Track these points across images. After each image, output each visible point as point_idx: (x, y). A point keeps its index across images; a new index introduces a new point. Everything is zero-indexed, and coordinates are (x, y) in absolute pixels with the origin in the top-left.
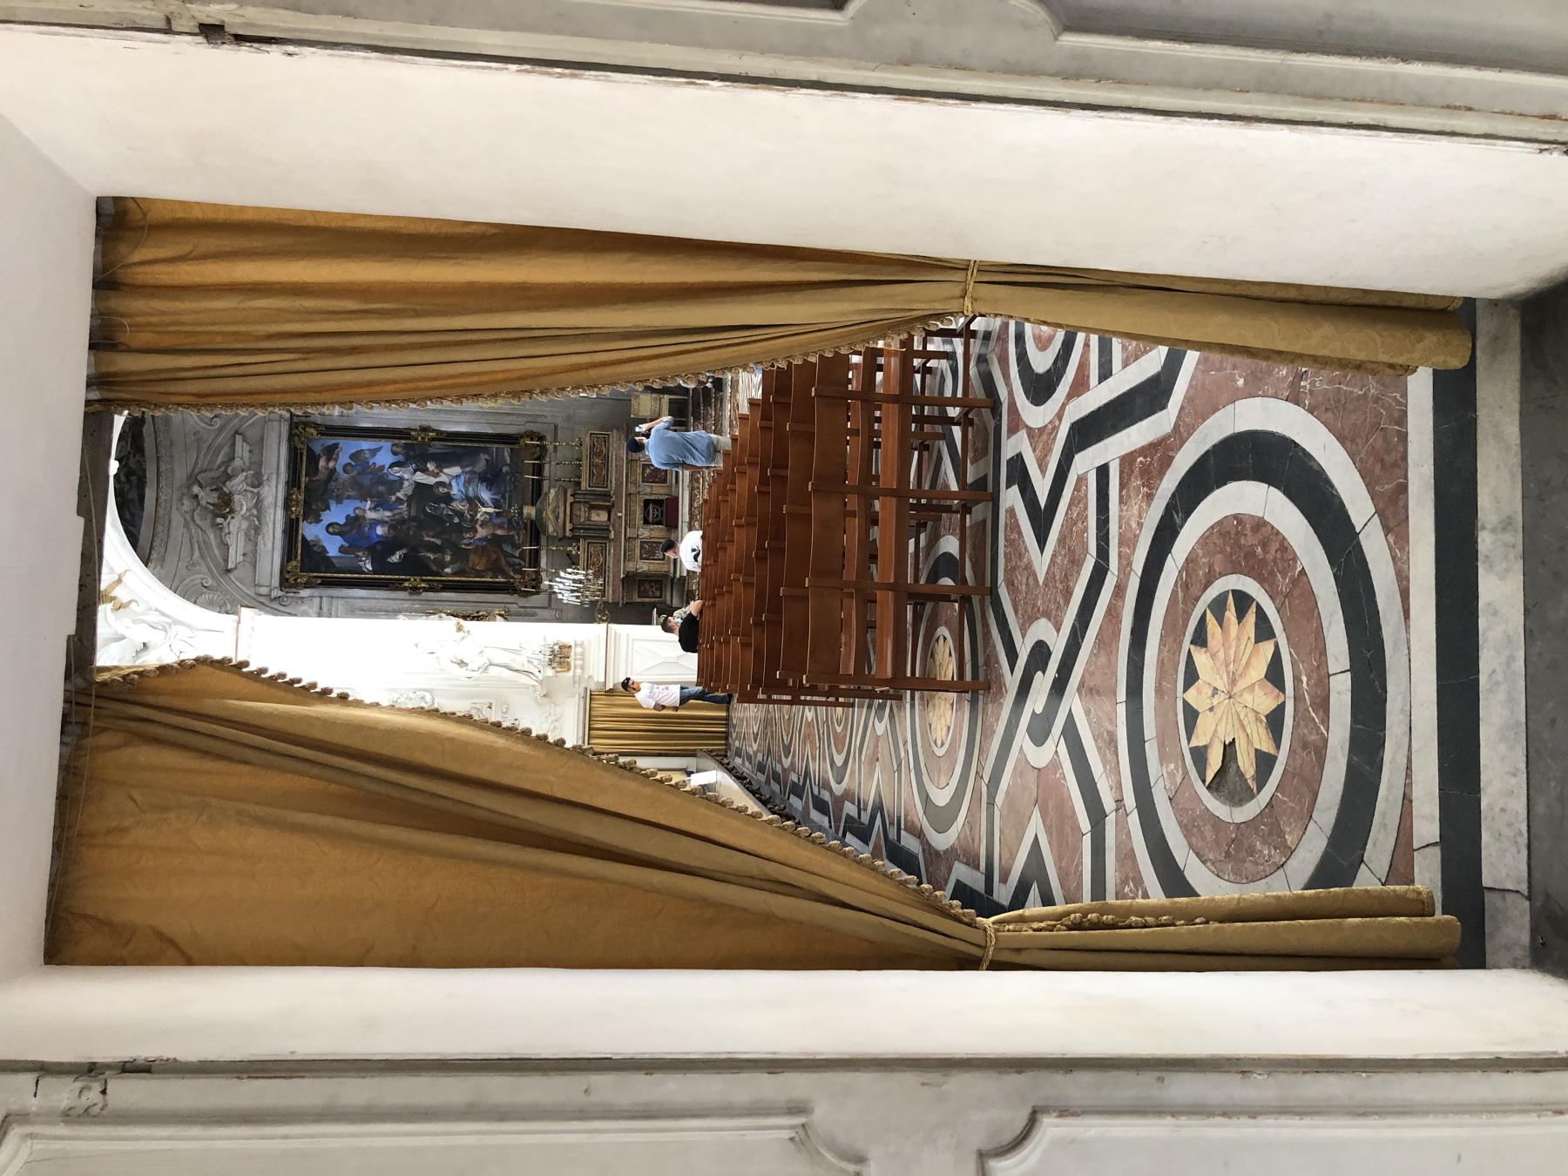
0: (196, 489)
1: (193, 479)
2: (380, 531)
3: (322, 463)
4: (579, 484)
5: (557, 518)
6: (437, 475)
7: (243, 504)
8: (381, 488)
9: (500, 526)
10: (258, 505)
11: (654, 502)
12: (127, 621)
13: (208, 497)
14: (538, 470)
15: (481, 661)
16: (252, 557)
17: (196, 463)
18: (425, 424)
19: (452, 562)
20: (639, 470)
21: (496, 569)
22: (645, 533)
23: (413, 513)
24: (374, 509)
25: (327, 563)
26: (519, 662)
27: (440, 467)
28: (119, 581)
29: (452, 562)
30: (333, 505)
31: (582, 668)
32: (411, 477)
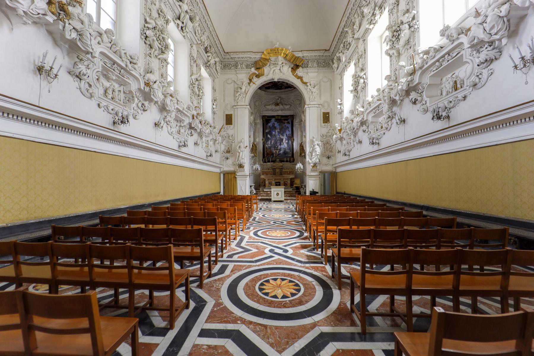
1: (281, 98)
2: (274, 133)
7: (278, 108)
10: (278, 110)
13: (279, 101)
14: (287, 161)
16: (268, 110)
21: (267, 154)
25: (267, 124)
26: (240, 158)
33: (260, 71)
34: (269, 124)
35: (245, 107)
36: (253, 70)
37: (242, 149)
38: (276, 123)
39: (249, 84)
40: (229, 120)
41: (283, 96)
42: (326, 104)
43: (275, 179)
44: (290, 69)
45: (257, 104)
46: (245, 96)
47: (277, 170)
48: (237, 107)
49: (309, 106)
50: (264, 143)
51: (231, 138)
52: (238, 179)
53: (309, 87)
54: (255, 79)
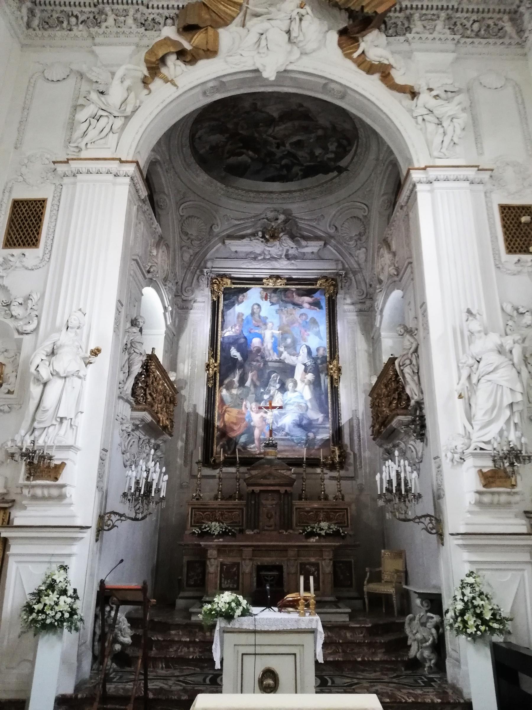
0: (282, 217)
1: (289, 219)
2: (256, 342)
3: (307, 299)
4: (300, 499)
5: (264, 477)
6: (303, 381)
7: (275, 249)
8: (289, 341)
9: (262, 432)
10: (273, 258)
11: (281, 577)
12: (127, 83)
15: (45, 373)
17: (302, 219)
18: (343, 371)
19: (232, 395)
20: (313, 560)
22: (247, 567)
23: (270, 364)
24: (273, 336)
25: (229, 306)
26: (45, 418)
27: (310, 383)
28: (166, 81)
29: (232, 395)
30: (277, 307)
31: (34, 497)
32: (300, 361)
33: (199, 38)
34: (238, 309)
35: (114, 166)
36: (170, 32)
37: (66, 362)
38: (266, 305)
39: (145, 82)
40: (26, 223)
41: (298, 208)
42: (509, 173)
43: (257, 550)
44: (333, 37)
45: (193, 232)
46: (118, 123)
47: (269, 504)
48: (74, 165)
49: (432, 173)
50: (211, 379)
51: (16, 310)
52: (14, 549)
53: (424, 98)
54: (174, 67)
